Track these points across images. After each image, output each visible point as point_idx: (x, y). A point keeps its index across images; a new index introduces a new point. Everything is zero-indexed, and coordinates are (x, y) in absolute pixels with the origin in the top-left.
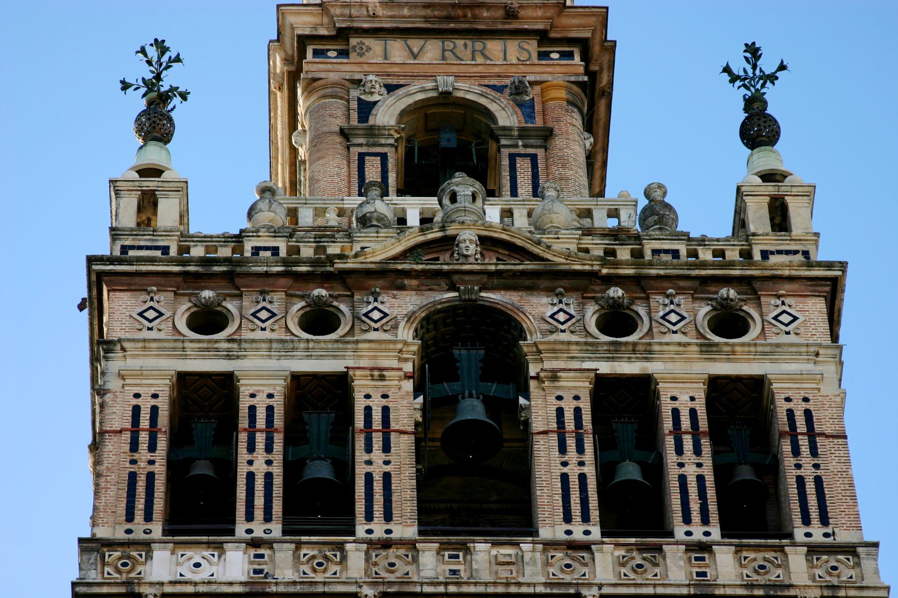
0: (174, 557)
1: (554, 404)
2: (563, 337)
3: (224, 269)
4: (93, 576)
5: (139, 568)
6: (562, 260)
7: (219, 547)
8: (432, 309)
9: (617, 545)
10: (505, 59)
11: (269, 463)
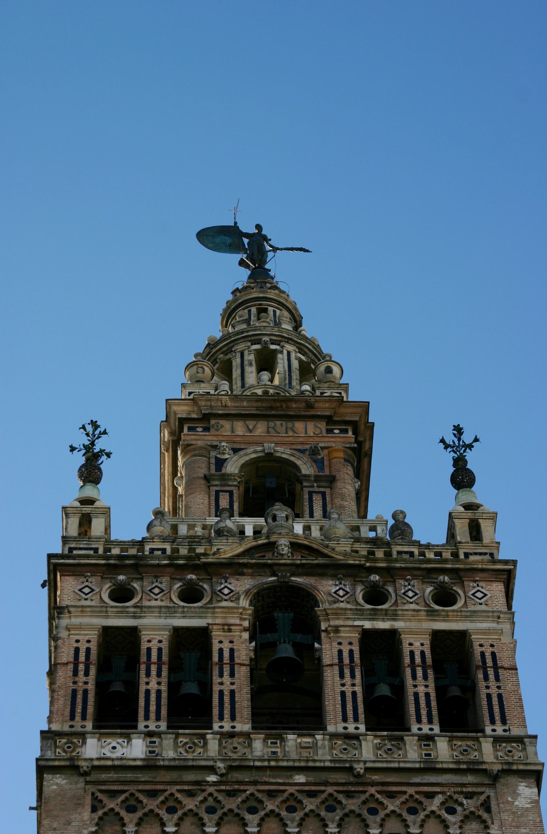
0: (100, 743)
1: (336, 647)
2: (342, 605)
3: (132, 562)
4: (49, 754)
5: (78, 750)
6: (341, 558)
7: (128, 737)
8: (261, 587)
9: (376, 736)
10: (306, 433)
11: (159, 683)
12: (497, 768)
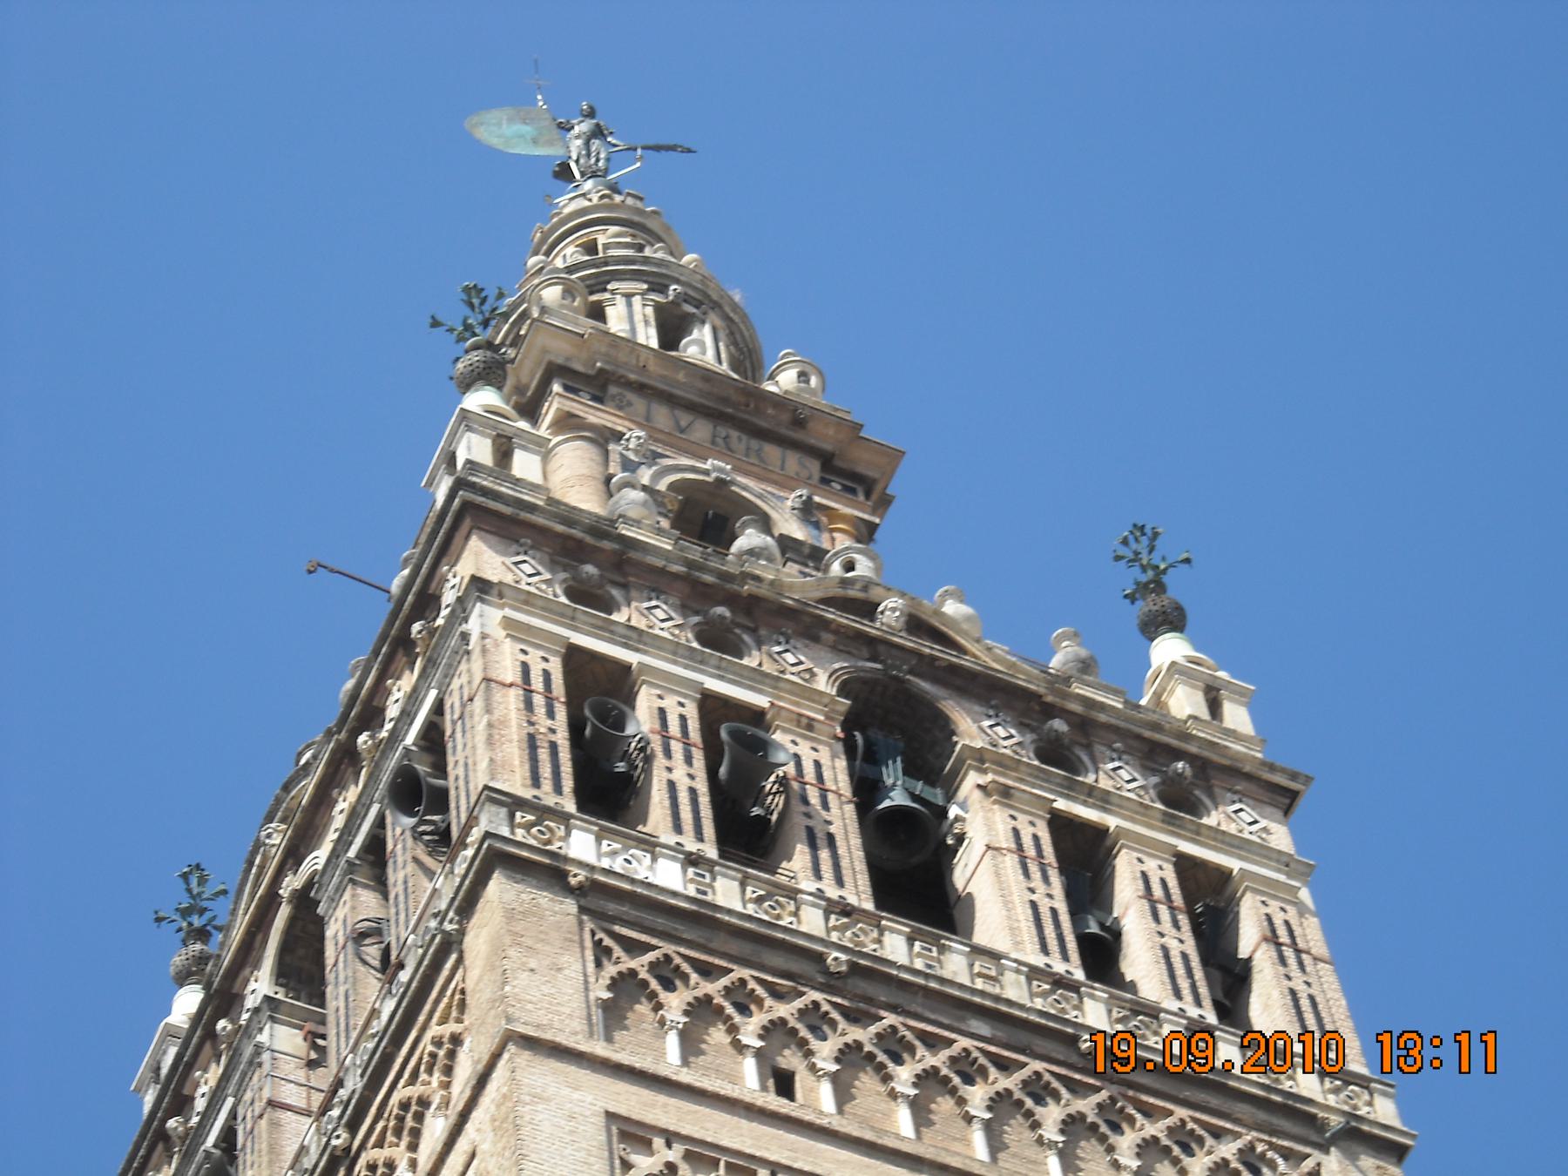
11: (692, 777)
12: (1336, 1121)
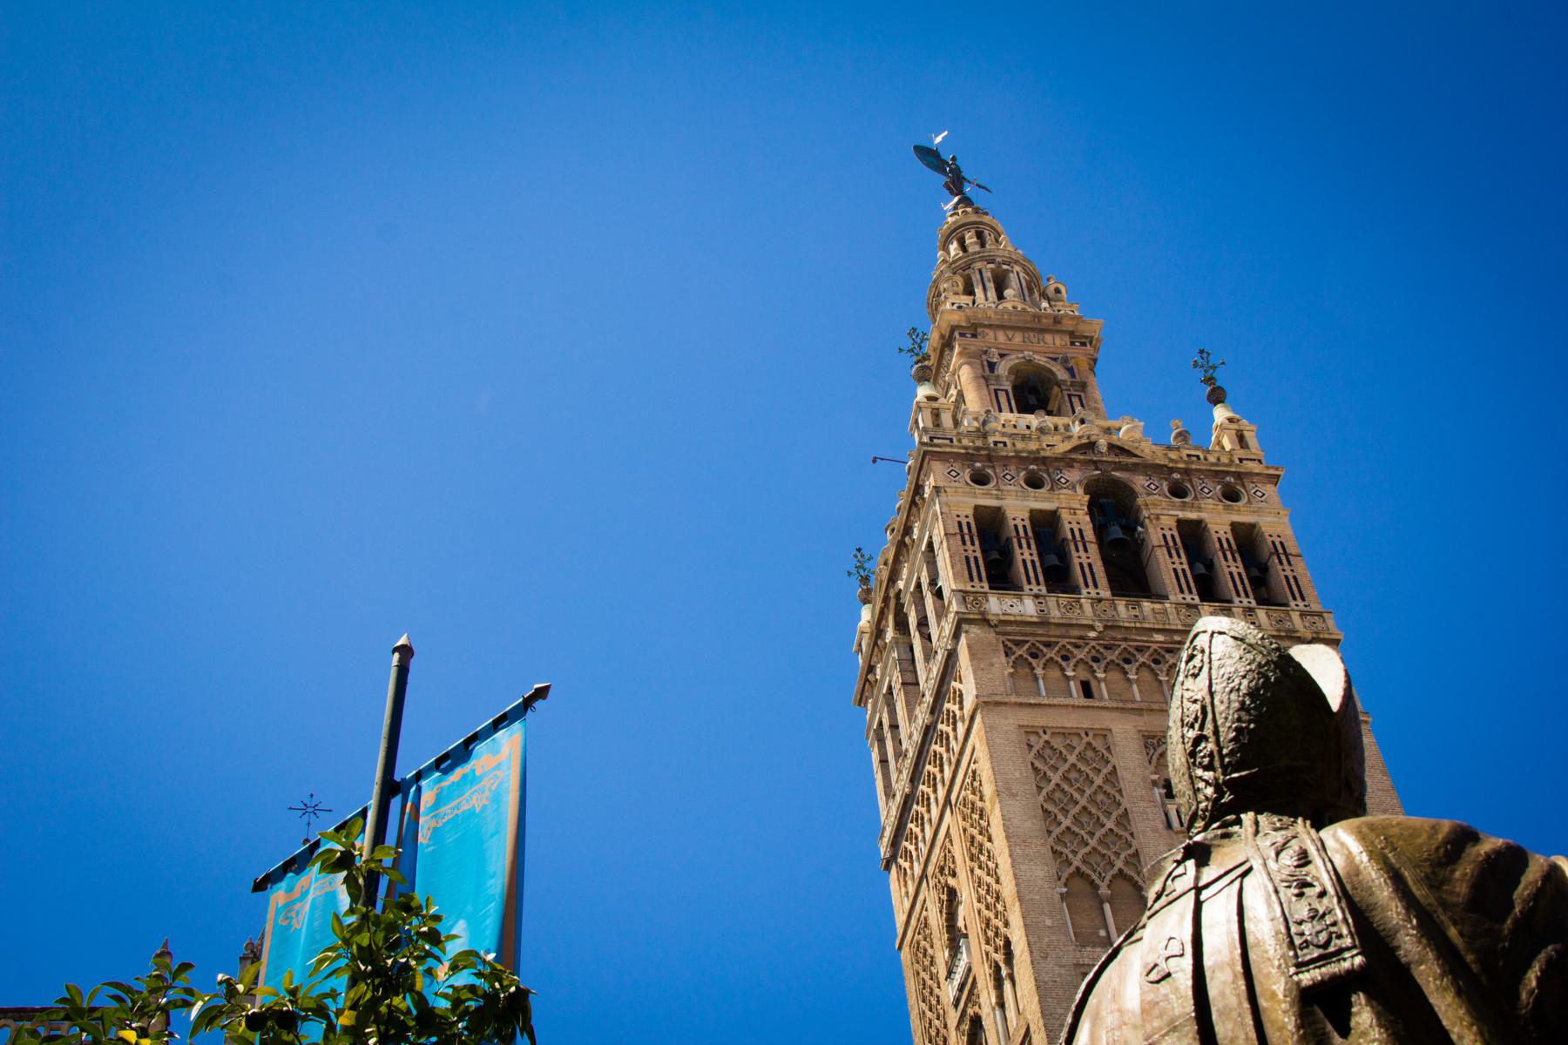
1: (1160, 533)
7: (1020, 598)
